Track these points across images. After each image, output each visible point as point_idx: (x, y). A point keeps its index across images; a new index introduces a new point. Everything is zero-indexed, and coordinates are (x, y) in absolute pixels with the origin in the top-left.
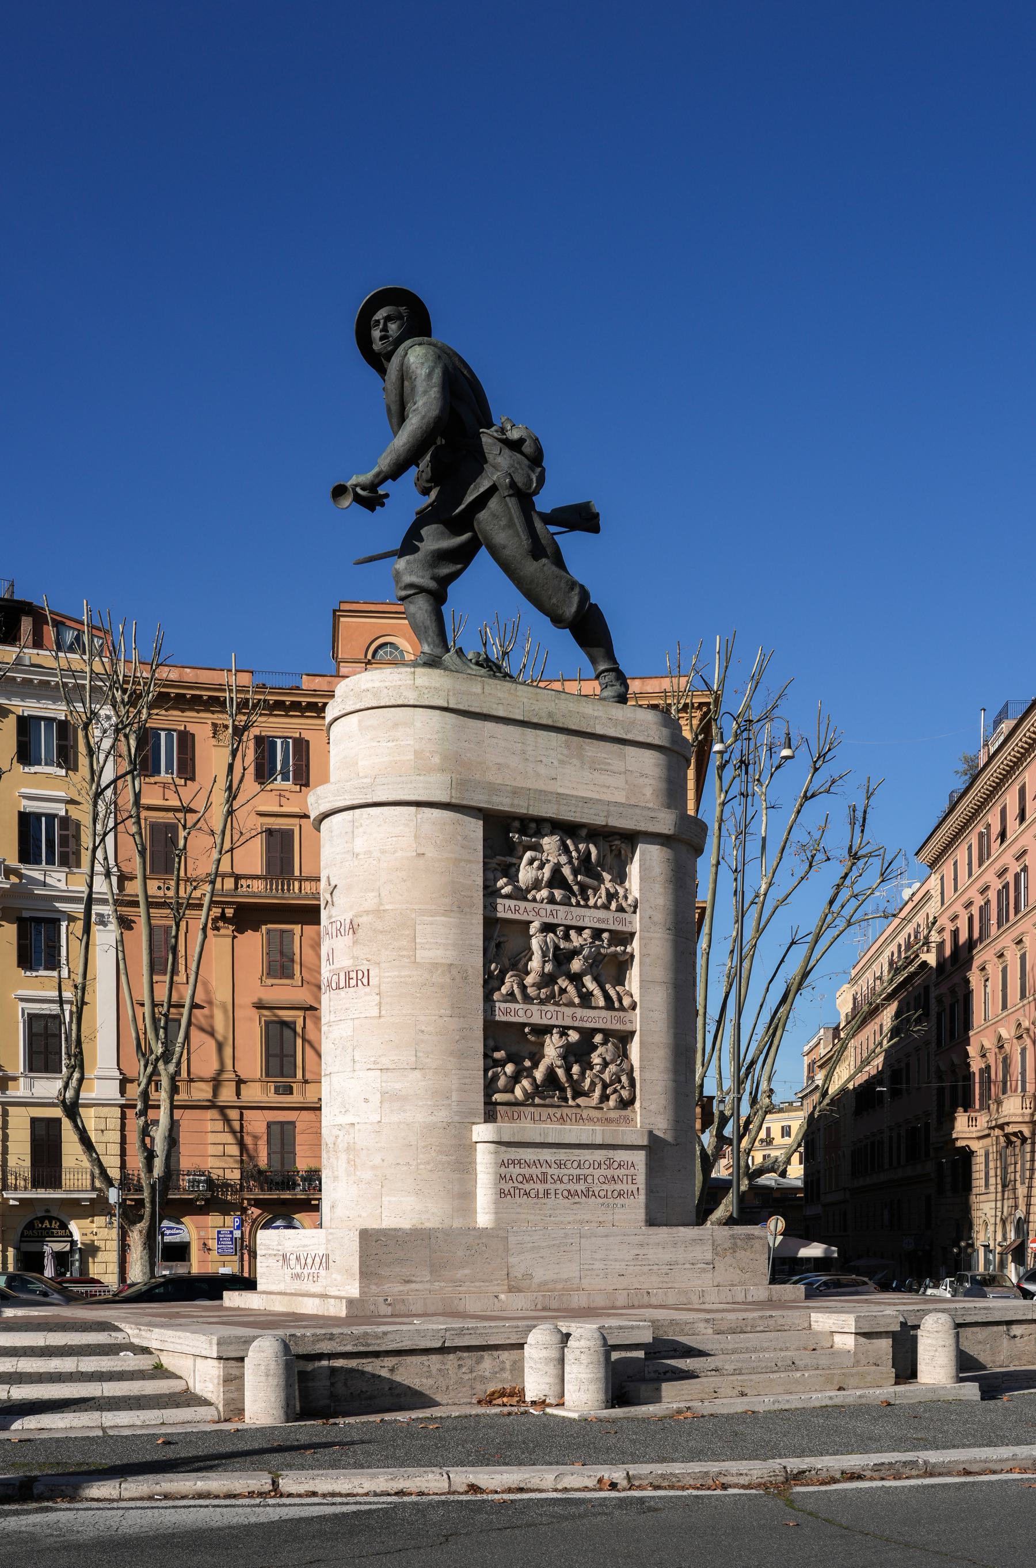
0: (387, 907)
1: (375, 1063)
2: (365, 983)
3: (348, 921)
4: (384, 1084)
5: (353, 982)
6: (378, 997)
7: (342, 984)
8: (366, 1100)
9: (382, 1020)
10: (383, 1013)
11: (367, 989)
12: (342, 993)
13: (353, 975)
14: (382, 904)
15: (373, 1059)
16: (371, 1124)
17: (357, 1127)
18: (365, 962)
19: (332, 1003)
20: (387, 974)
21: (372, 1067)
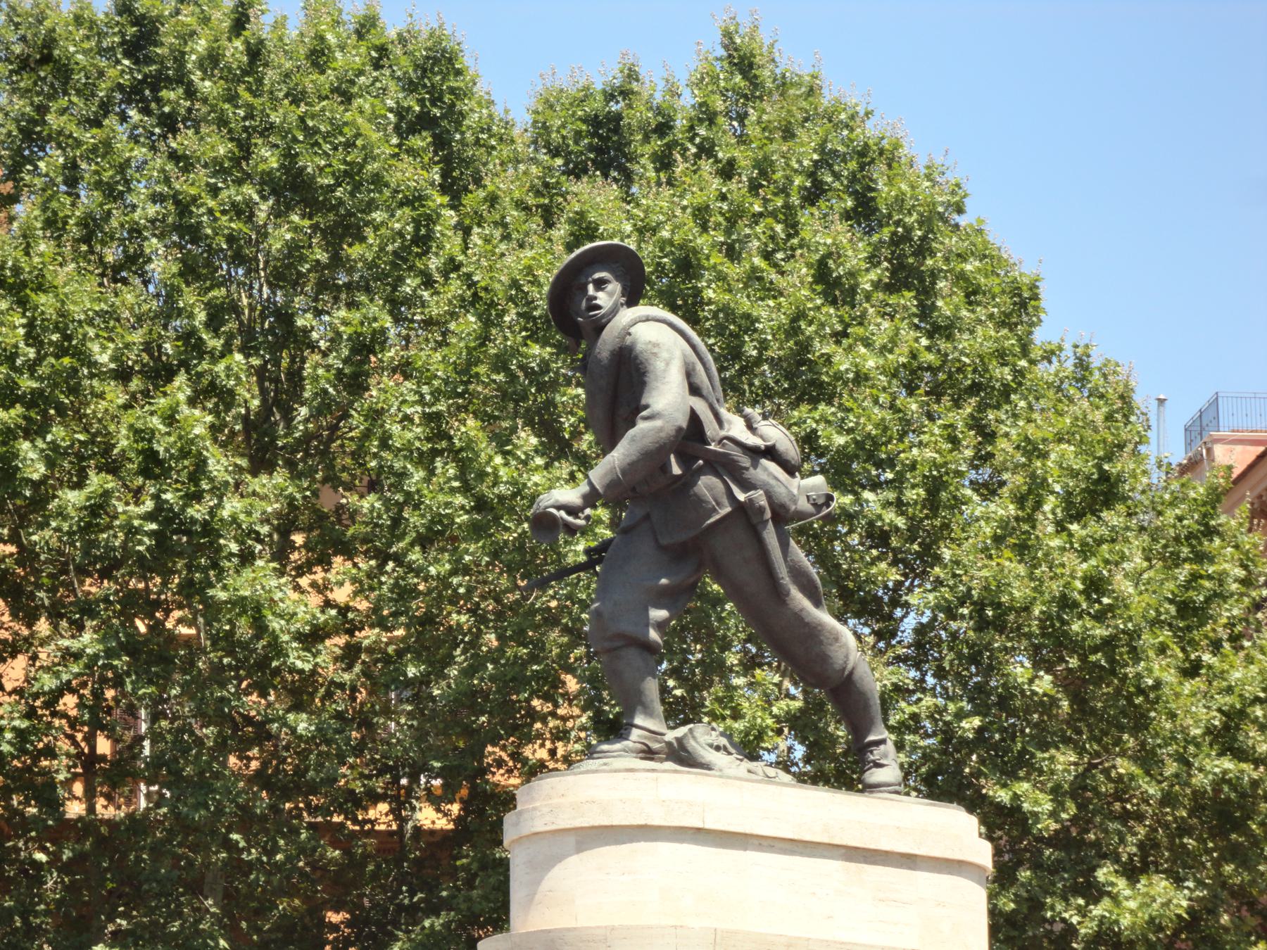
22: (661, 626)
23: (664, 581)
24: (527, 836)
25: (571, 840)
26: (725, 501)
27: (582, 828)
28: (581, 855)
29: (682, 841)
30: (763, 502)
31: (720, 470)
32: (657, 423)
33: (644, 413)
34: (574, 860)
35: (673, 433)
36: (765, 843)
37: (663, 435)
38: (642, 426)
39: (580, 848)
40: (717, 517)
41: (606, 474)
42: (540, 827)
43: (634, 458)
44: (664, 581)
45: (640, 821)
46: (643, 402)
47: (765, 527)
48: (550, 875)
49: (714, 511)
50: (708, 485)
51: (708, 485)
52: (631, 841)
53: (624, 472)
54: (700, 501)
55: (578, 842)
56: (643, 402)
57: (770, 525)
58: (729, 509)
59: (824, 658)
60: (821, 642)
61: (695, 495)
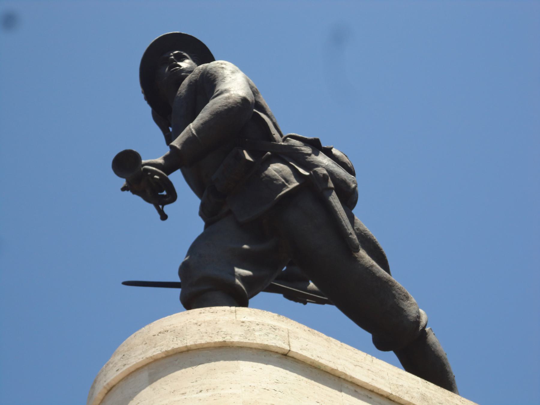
22: (243, 279)
23: (245, 246)
25: (145, 375)
26: (292, 179)
28: (157, 384)
29: (267, 363)
30: (325, 172)
31: (287, 159)
34: (147, 393)
35: (240, 101)
36: (358, 390)
37: (231, 101)
39: (152, 380)
40: (287, 190)
43: (207, 118)
44: (245, 246)
45: (219, 339)
47: (330, 195)
49: (283, 186)
50: (276, 169)
51: (276, 169)
52: (209, 361)
54: (271, 180)
57: (334, 193)
59: (397, 312)
60: (394, 296)
61: (267, 176)
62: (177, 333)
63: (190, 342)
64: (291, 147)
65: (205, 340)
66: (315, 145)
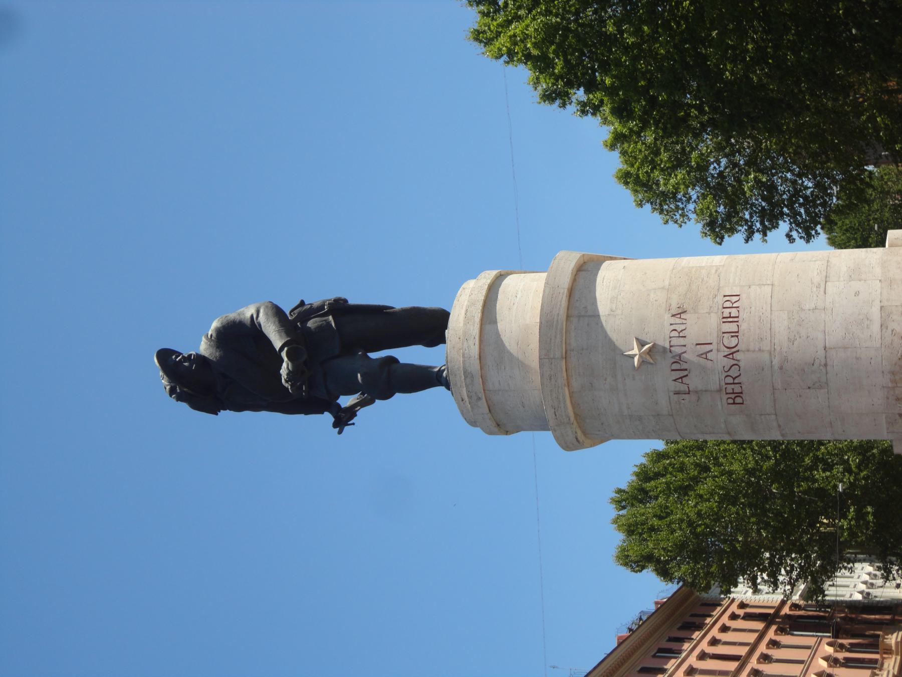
0: (667, 283)
1: (818, 287)
2: (734, 299)
3: (673, 320)
4: (842, 279)
5: (734, 312)
6: (753, 287)
7: (733, 327)
8: (857, 294)
9: (776, 283)
10: (769, 282)
11: (743, 296)
12: (744, 326)
13: (726, 314)
14: (663, 288)
15: (815, 289)
16: (882, 288)
17: (885, 303)
18: (716, 300)
19: (751, 348)
20: (731, 281)
21: (822, 289)
24: (481, 369)
25: (488, 327)
27: (482, 320)
32: (262, 311)
33: (255, 316)
34: (501, 326)
38: (262, 319)
39: (494, 322)
41: (281, 336)
42: (475, 350)
46: (248, 322)
48: (507, 344)
49: (329, 324)
50: (311, 324)
52: (497, 293)
53: (282, 326)
54: (320, 328)
55: (490, 323)
56: (248, 322)
58: (330, 318)
61: (315, 329)
62: (472, 303)
63: (481, 298)
64: (299, 313)
65: (484, 292)
66: (302, 303)
